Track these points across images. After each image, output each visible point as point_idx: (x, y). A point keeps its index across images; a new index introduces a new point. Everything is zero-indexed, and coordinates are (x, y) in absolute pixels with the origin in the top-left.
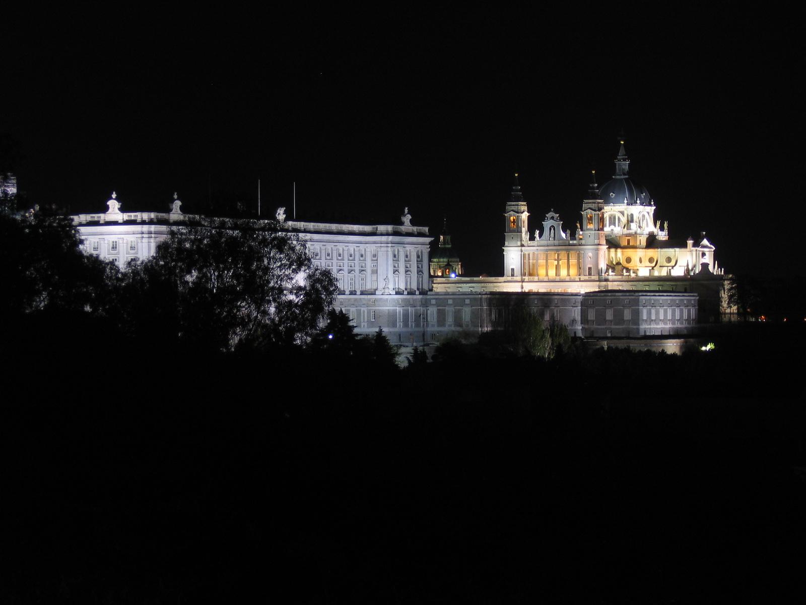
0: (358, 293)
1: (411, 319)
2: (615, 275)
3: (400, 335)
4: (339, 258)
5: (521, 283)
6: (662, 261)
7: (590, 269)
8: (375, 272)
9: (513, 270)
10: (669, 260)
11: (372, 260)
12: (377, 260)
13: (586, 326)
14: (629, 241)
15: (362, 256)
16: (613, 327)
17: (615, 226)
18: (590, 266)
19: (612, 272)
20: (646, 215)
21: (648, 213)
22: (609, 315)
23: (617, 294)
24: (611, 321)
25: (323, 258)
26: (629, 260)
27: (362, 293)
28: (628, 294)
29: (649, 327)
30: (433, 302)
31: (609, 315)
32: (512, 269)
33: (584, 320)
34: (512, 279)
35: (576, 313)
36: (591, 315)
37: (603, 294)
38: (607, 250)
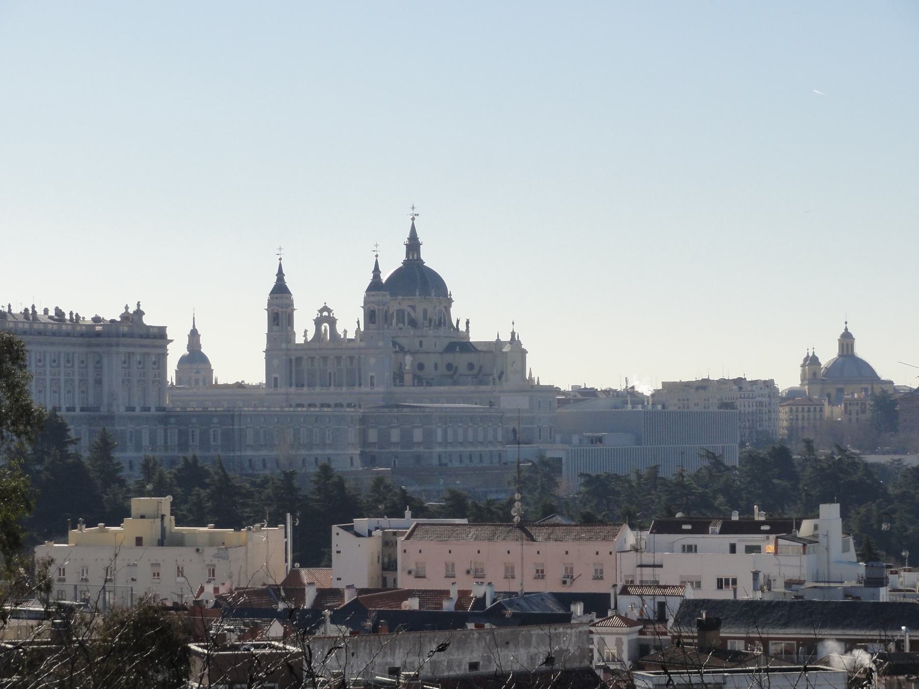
0: (78, 409)
1: (145, 442)
2: (403, 386)
3: (131, 462)
4: (54, 365)
5: (285, 397)
6: (463, 369)
7: (372, 377)
8: (99, 382)
9: (276, 379)
10: (471, 366)
11: (96, 368)
12: (101, 367)
13: (367, 450)
14: (421, 343)
15: (82, 362)
16: (399, 450)
17: (404, 325)
18: (371, 374)
19: (400, 382)
20: (444, 310)
21: (446, 307)
22: (395, 435)
23: (405, 410)
24: (398, 443)
25: (48, 365)
26: (421, 366)
27: (82, 410)
28: (418, 410)
29: (445, 450)
30: (172, 420)
31: (395, 435)
32: (274, 378)
33: (364, 442)
34: (274, 390)
35: (352, 434)
36: (373, 436)
37: (386, 410)
38: (393, 356)
